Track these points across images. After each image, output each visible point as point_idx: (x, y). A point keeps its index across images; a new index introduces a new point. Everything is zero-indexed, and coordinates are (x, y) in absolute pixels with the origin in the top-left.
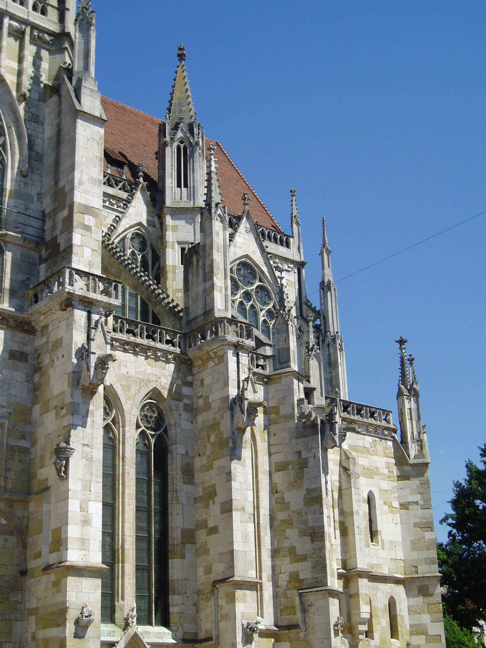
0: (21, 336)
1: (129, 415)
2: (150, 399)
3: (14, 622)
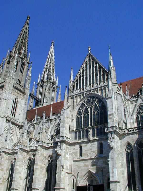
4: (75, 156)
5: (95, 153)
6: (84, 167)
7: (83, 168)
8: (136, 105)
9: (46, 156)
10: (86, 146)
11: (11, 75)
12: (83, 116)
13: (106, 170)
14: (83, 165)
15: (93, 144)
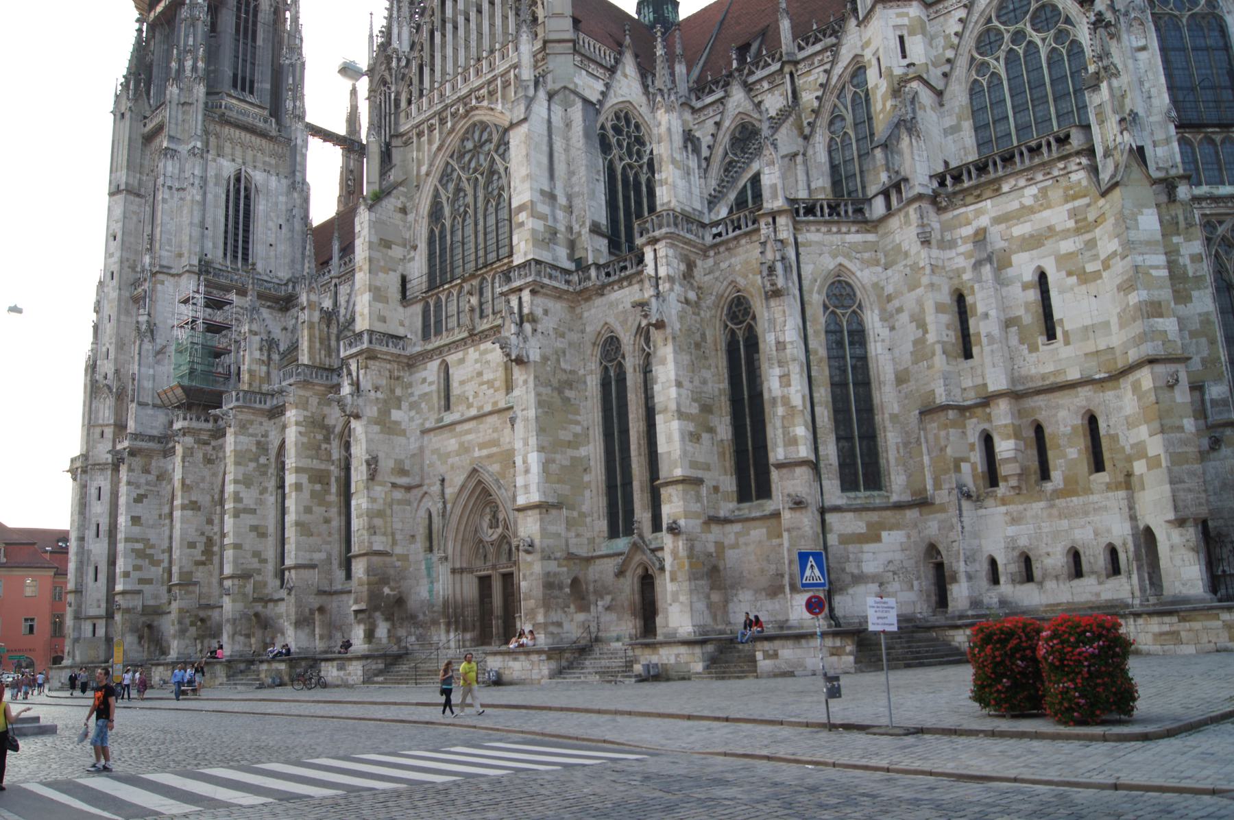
5: (492, 391)
6: (458, 454)
8: (718, 124)
9: (334, 427)
11: (189, 64)
12: (448, 224)
15: (486, 352)
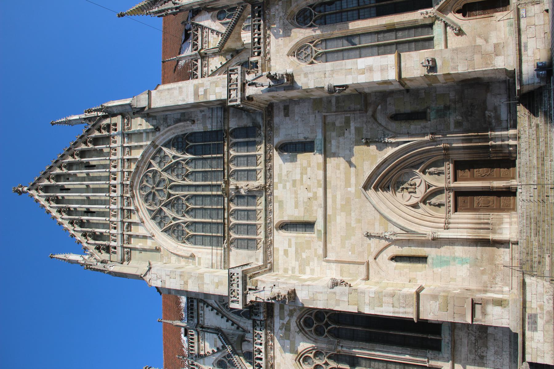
0: (275, 111)
1: (306, 34)
2: (294, 19)
3: (437, 93)
4: (310, 249)
5: (309, 169)
6: (349, 214)
7: (353, 214)
10: (281, 203)
13: (365, 126)
14: (343, 214)
15: (280, 175)
